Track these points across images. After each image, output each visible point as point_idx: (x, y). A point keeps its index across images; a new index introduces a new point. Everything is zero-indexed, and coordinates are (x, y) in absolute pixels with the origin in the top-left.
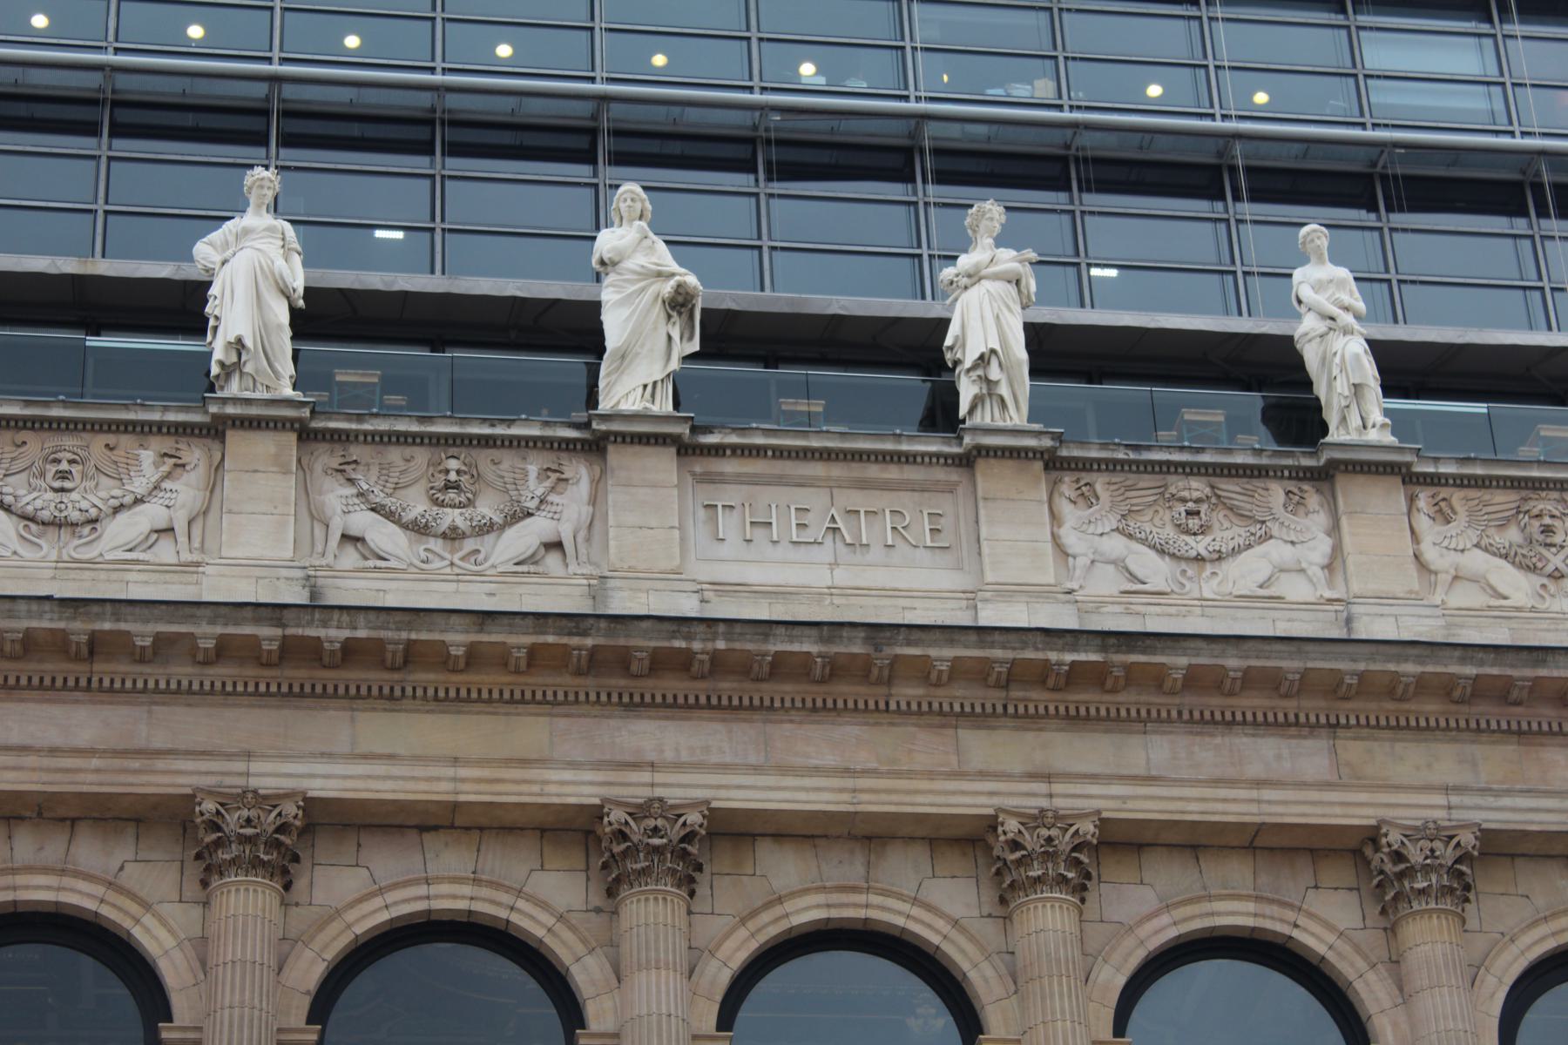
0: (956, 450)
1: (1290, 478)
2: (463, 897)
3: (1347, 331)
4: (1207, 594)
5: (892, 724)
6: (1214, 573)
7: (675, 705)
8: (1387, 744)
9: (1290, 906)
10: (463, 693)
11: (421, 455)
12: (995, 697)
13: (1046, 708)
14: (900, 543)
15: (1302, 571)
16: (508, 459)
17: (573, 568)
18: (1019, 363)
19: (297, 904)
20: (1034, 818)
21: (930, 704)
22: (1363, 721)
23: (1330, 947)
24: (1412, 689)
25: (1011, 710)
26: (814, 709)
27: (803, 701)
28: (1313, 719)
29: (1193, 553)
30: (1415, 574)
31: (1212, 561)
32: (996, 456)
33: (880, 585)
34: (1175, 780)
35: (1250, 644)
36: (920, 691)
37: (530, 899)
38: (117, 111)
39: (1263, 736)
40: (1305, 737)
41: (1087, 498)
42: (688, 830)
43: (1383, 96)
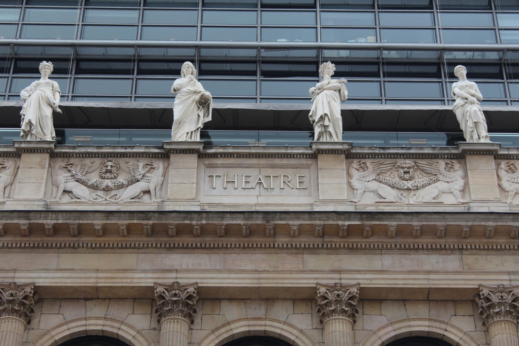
0: (310, 152)
1: (448, 158)
2: (100, 325)
3: (472, 103)
4: (411, 203)
5: (276, 253)
6: (414, 195)
7: (187, 248)
8: (484, 256)
9: (444, 322)
10: (102, 245)
11: (98, 161)
12: (318, 241)
13: (340, 245)
14: (286, 187)
15: (452, 192)
16: (132, 162)
17: (154, 199)
18: (338, 119)
19: (33, 329)
20: (332, 287)
21: (292, 245)
22: (473, 247)
23: (461, 339)
24: (493, 233)
25: (325, 246)
26: (244, 248)
27: (240, 245)
28: (452, 247)
29: (406, 187)
30: (498, 192)
31: (414, 190)
32: (325, 153)
33: (276, 203)
34: (393, 272)
35: (423, 216)
36: (287, 239)
37: (127, 325)
38: (19, 63)
39: (431, 254)
40: (449, 254)
41: (363, 168)
42: (189, 294)
43: (505, 35)
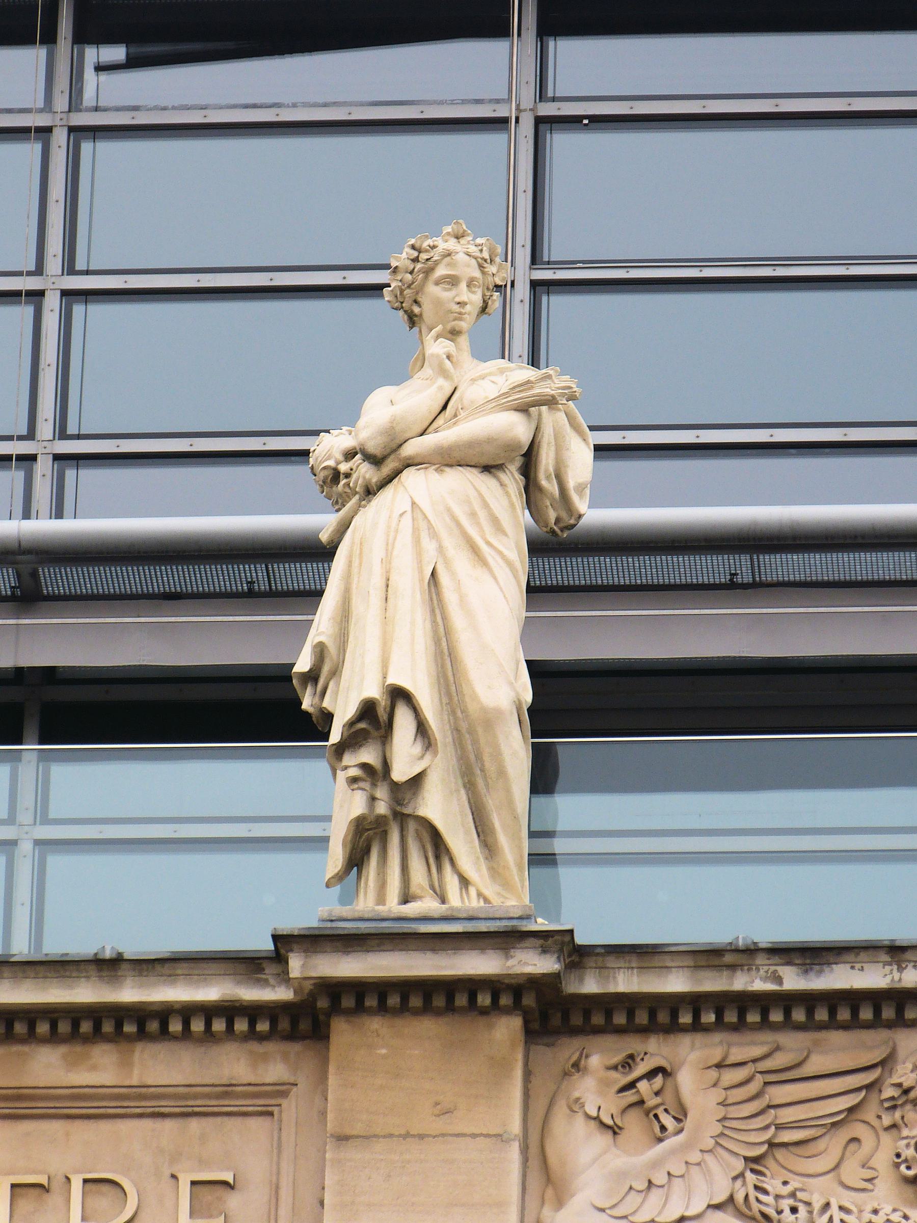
41: (650, 1109)
